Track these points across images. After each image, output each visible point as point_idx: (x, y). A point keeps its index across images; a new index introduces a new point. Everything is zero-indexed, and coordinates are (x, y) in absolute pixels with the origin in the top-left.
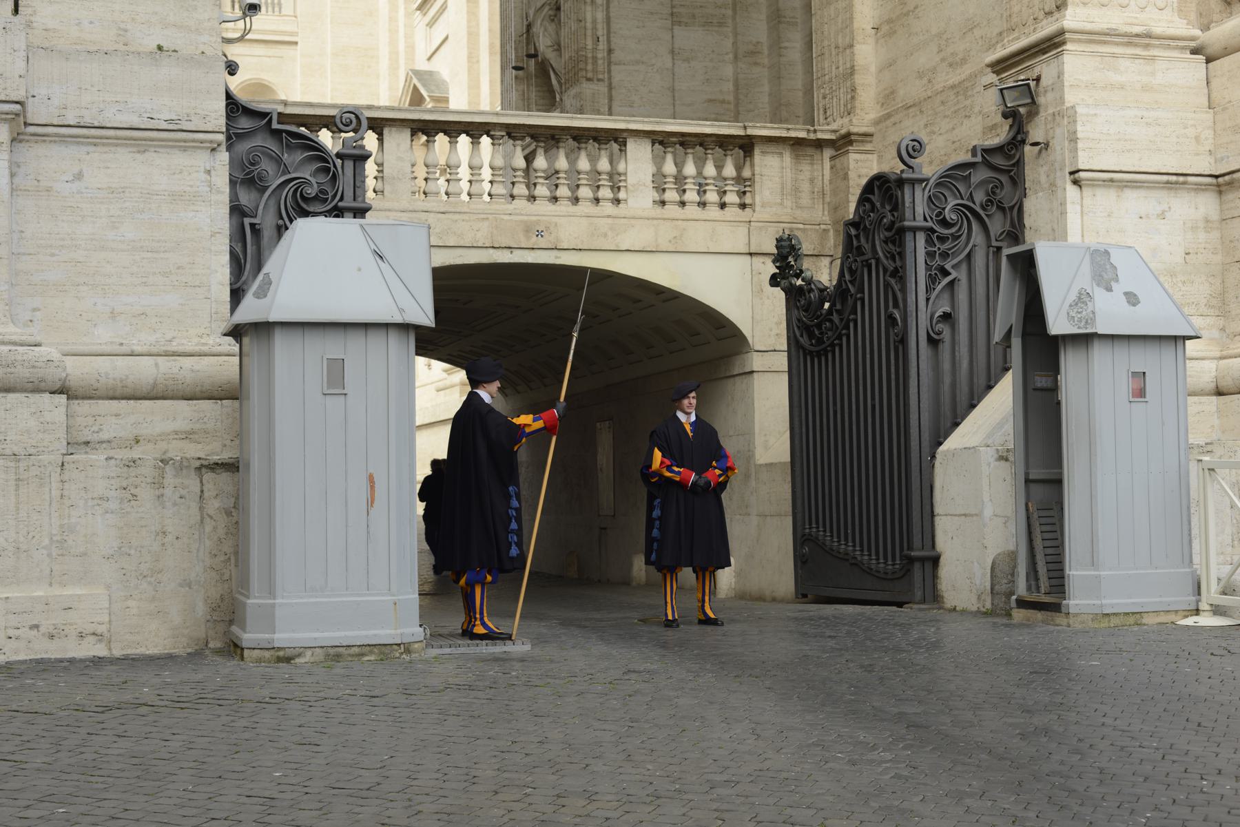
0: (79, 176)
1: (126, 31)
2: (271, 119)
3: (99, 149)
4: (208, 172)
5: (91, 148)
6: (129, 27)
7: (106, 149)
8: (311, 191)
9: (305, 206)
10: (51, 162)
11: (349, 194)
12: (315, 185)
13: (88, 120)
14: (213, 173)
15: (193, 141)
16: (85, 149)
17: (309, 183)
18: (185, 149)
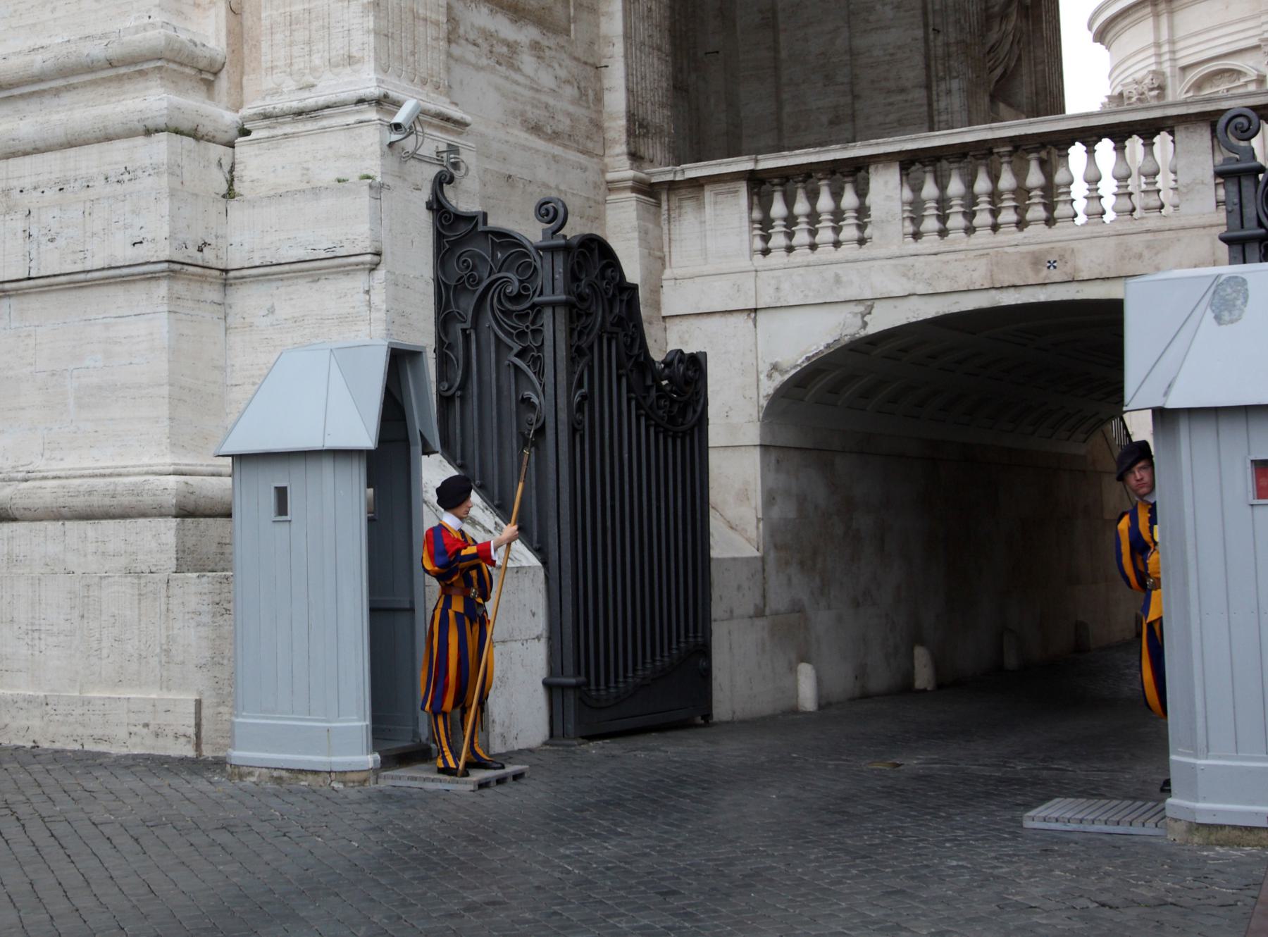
0: (272, 310)
1: (308, 169)
2: (477, 224)
3: (286, 283)
4: (368, 292)
5: (280, 283)
6: (310, 165)
7: (290, 282)
8: (513, 288)
9: (509, 306)
10: (248, 300)
11: (548, 290)
12: (517, 284)
13: (268, 260)
14: (372, 292)
15: (350, 265)
16: (275, 284)
17: (508, 282)
18: (347, 273)
